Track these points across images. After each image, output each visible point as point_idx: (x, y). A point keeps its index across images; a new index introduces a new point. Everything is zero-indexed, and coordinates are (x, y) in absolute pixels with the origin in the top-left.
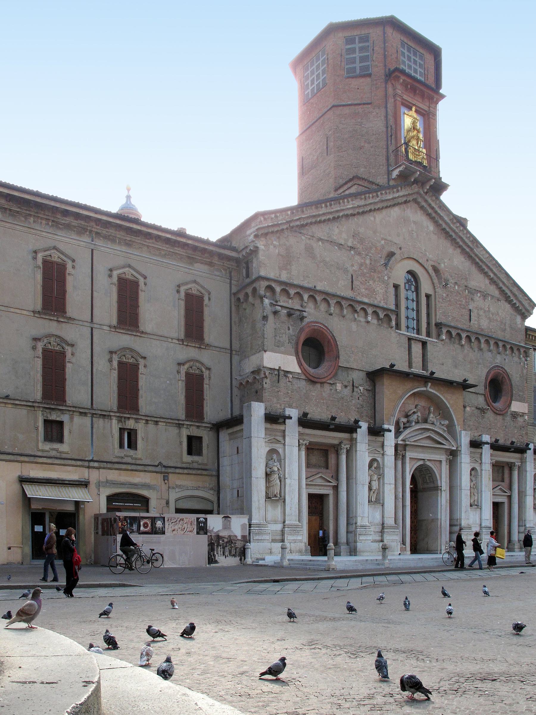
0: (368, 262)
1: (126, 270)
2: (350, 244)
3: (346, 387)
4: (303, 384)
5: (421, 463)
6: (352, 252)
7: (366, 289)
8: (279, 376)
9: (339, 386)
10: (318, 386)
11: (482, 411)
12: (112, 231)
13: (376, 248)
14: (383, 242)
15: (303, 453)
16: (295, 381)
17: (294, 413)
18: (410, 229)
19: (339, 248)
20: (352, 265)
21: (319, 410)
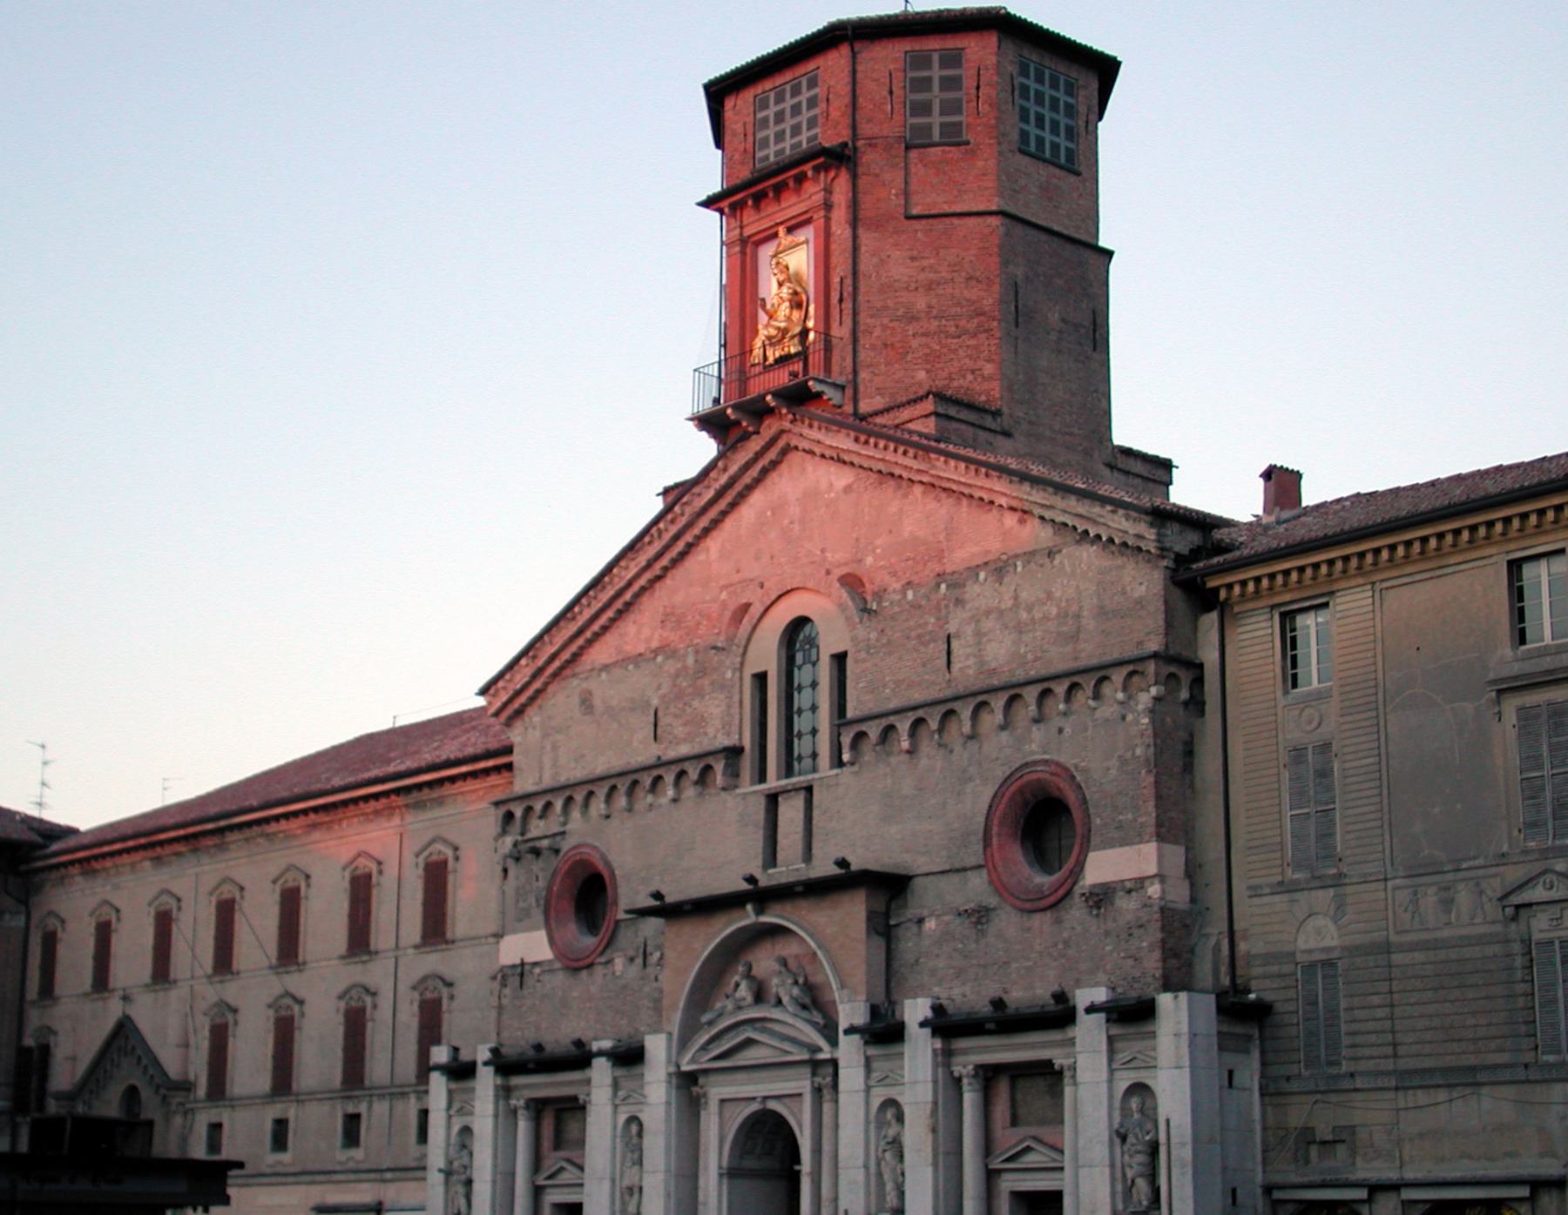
0: (690, 660)
1: (439, 846)
2: (655, 644)
3: (632, 960)
4: (560, 978)
5: (755, 1107)
6: (659, 659)
7: (685, 725)
8: (522, 975)
9: (619, 963)
10: (584, 973)
11: (979, 916)
12: (415, 795)
13: (709, 617)
14: (724, 595)
15: (523, 1126)
16: (546, 977)
17: (483, 1054)
18: (786, 522)
19: (637, 666)
20: (659, 688)
21: (583, 1024)
